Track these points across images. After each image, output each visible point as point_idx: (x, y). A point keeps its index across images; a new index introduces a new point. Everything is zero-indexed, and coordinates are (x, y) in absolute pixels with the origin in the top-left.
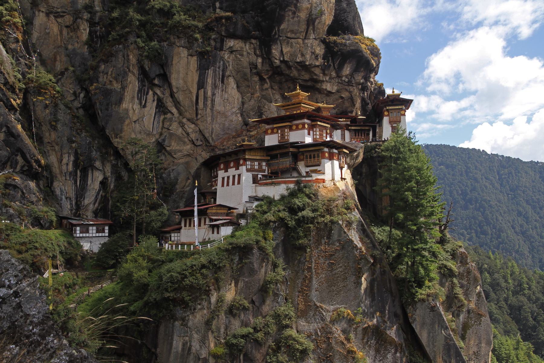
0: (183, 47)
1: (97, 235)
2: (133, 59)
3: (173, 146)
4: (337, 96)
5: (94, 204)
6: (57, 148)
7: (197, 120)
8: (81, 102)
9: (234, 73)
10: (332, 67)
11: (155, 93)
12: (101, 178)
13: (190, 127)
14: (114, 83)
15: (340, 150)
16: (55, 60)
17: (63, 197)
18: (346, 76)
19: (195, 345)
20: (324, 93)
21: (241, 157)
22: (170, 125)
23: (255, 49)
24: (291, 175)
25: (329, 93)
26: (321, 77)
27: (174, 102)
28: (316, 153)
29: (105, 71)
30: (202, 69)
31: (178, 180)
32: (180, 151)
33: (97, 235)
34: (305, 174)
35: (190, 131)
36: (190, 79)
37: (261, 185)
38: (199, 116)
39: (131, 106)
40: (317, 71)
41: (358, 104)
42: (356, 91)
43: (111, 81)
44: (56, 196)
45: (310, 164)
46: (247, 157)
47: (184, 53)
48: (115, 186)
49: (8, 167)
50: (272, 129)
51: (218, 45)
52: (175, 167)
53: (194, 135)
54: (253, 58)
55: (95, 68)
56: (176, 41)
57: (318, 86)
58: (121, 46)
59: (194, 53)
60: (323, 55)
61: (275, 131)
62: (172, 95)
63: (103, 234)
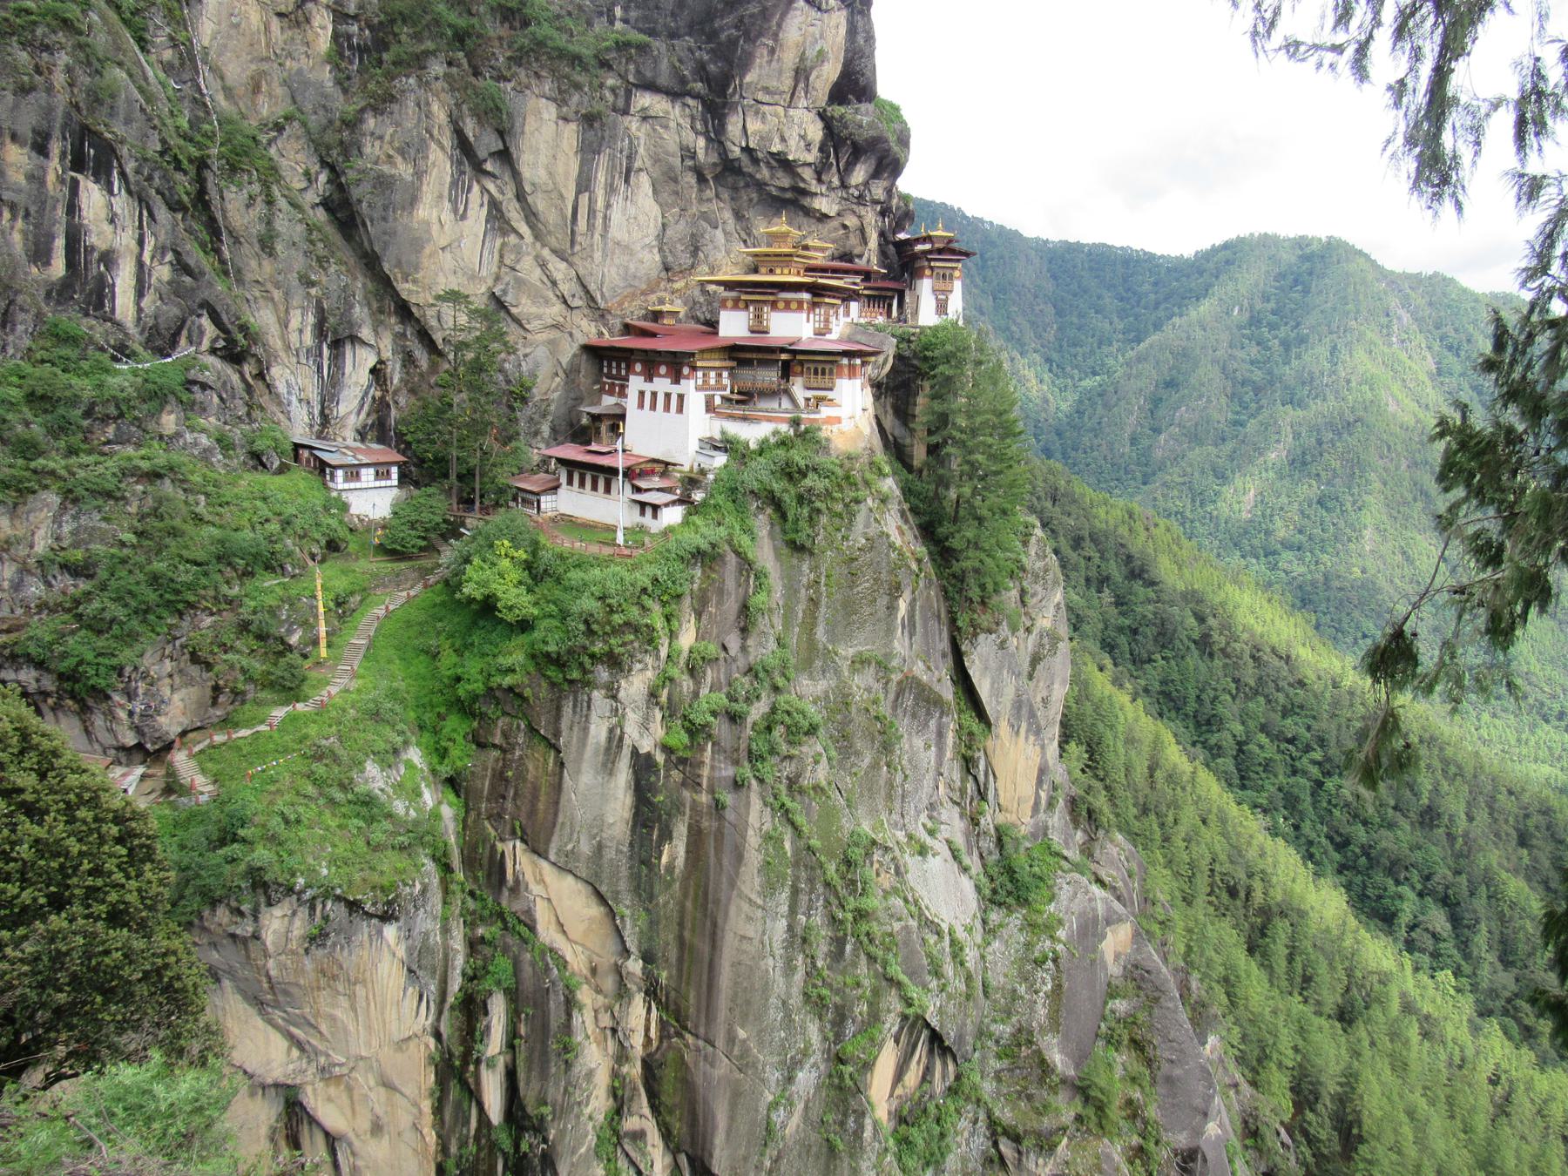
1: (378, 484)
2: (440, 114)
3: (523, 306)
4: (835, 223)
5: (359, 413)
6: (277, 295)
9: (648, 164)
10: (834, 168)
11: (484, 190)
12: (372, 361)
13: (559, 268)
14: (399, 159)
16: (256, 89)
17: (294, 399)
18: (856, 187)
19: (632, 731)
22: (518, 261)
23: (693, 118)
25: (824, 217)
26: (814, 187)
28: (827, 367)
29: (378, 132)
30: (588, 151)
32: (539, 317)
34: (802, 403)
35: (558, 276)
36: (560, 169)
38: (577, 248)
39: (435, 214)
40: (807, 174)
43: (390, 156)
44: (278, 395)
46: (699, 364)
47: (549, 111)
48: (401, 380)
49: (183, 341)
50: (736, 301)
51: (621, 103)
52: (528, 350)
54: (689, 137)
55: (352, 124)
57: (806, 201)
58: (411, 81)
59: (571, 116)
61: (741, 305)
62: (520, 196)
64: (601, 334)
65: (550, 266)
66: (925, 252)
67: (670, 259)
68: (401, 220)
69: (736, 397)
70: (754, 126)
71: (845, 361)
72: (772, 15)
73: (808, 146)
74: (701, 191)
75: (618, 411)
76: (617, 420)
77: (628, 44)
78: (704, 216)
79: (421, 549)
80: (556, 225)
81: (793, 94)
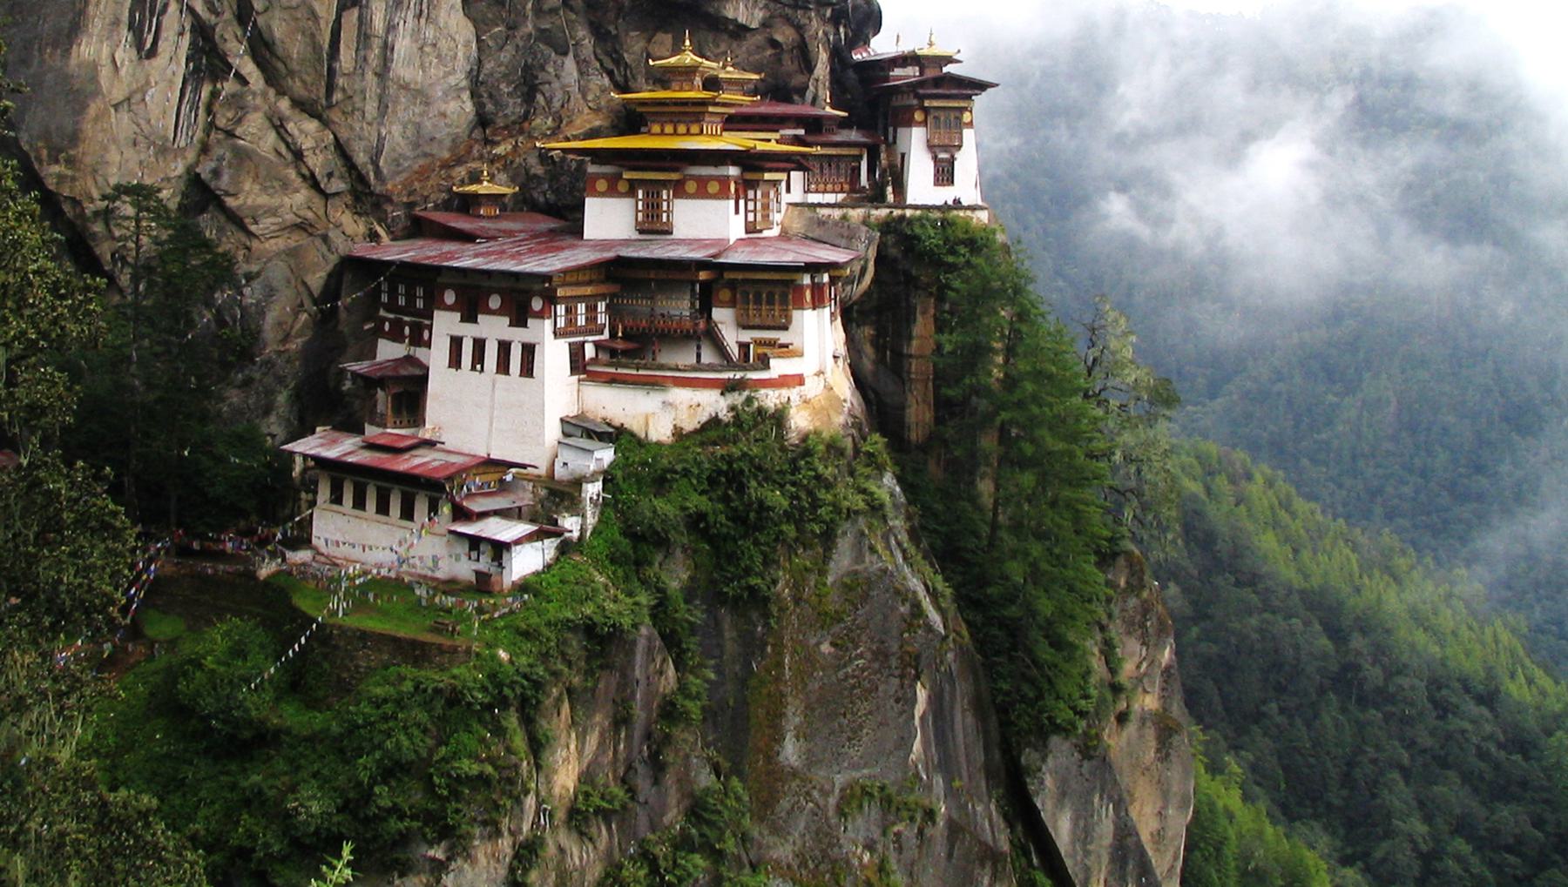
3: (248, 195)
7: (330, 106)
13: (306, 131)
15: (837, 273)
20: (726, 30)
21: (537, 287)
22: (239, 121)
24: (699, 356)
25: (740, 31)
28: (778, 290)
32: (273, 212)
34: (734, 351)
35: (306, 144)
37: (594, 377)
39: (105, 51)
41: (819, 65)
42: (814, 22)
45: (757, 321)
46: (560, 292)
52: (254, 268)
53: (321, 158)
61: (622, 187)
64: (373, 236)
65: (290, 126)
66: (913, 88)
67: (490, 107)
69: (620, 345)
71: (807, 280)
75: (418, 372)
76: (410, 394)
78: (544, 36)
80: (302, 61)
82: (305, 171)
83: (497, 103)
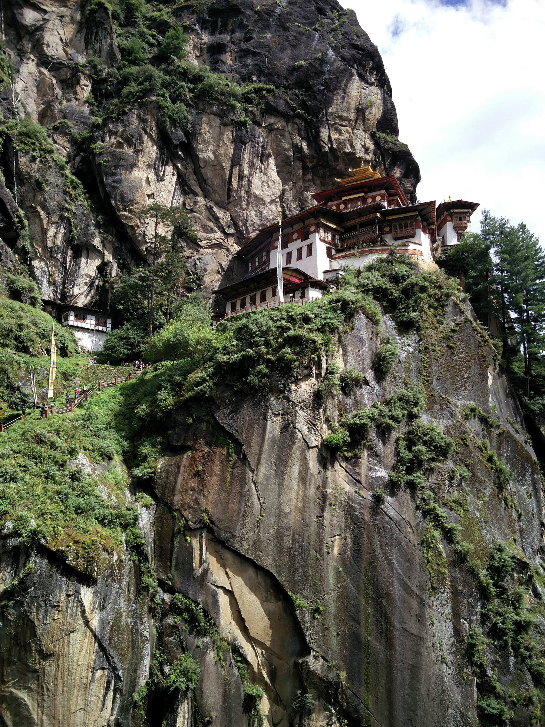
0: (215, 115)
7: (229, 203)
8: (76, 167)
11: (175, 167)
12: (98, 262)
27: (198, 180)
28: (408, 222)
30: (239, 142)
31: (206, 270)
33: (97, 328)
38: (232, 199)
54: (297, 139)
56: (206, 107)
60: (374, 150)
62: (197, 172)
63: (105, 329)
67: (287, 212)
68: (124, 175)
70: (334, 136)
72: (342, 80)
73: (367, 151)
74: (304, 174)
77: (261, 89)
79: (127, 355)
81: (356, 122)
82: (219, 224)
83: (290, 210)
